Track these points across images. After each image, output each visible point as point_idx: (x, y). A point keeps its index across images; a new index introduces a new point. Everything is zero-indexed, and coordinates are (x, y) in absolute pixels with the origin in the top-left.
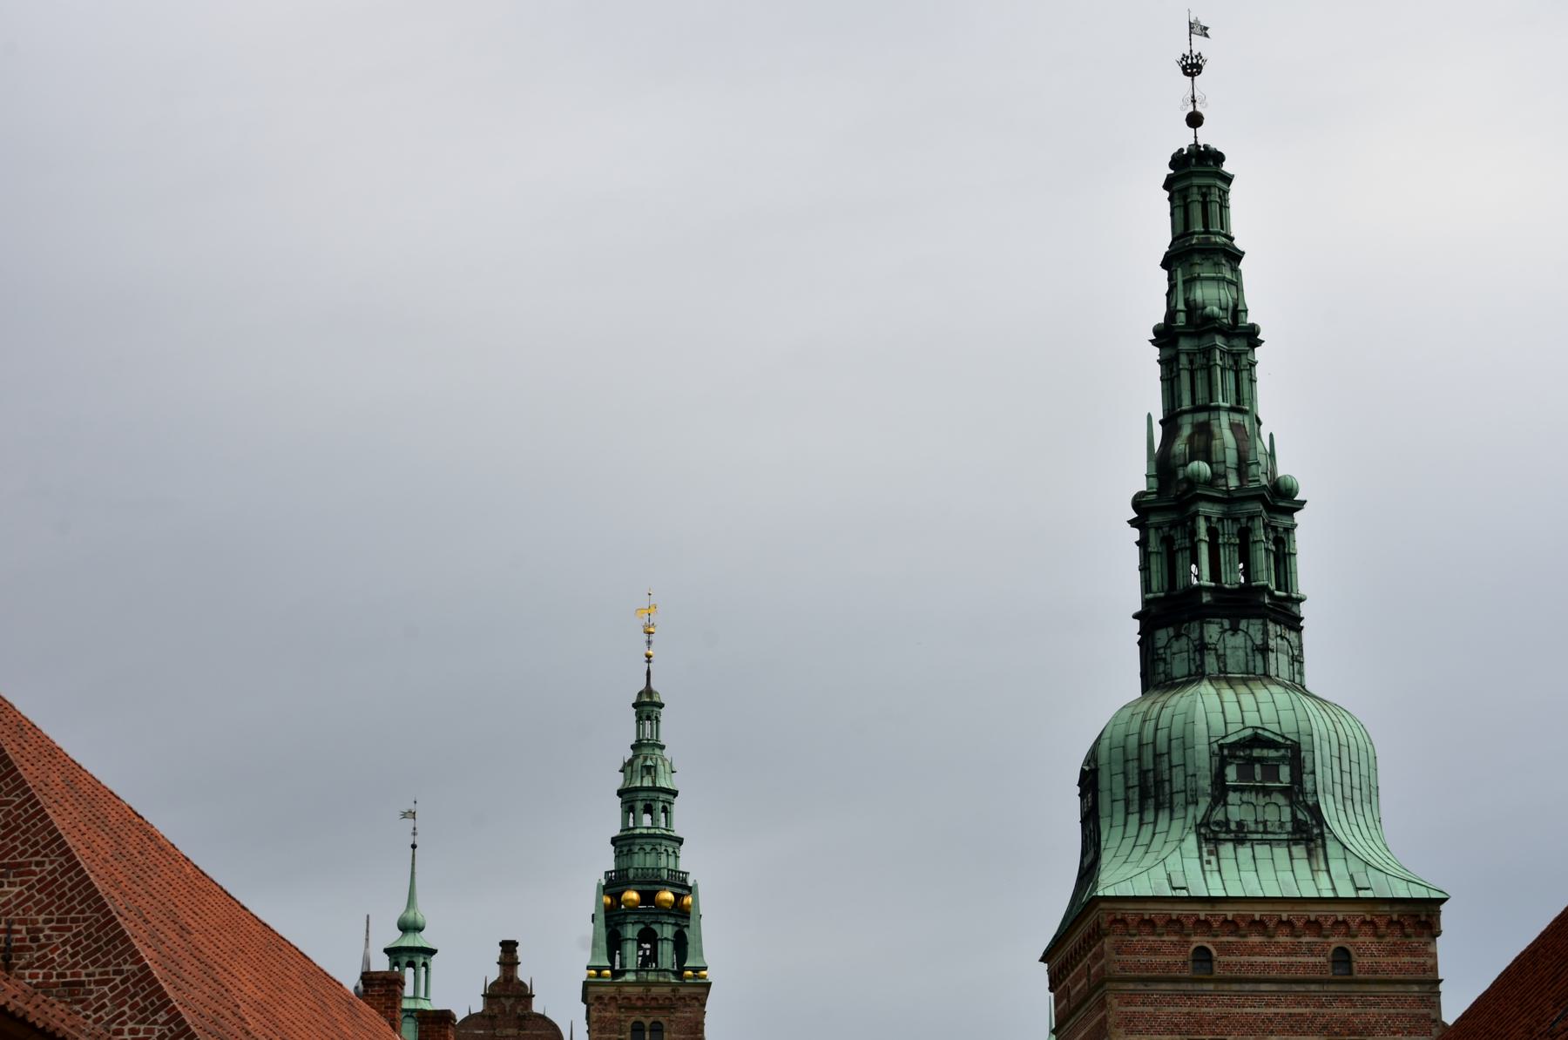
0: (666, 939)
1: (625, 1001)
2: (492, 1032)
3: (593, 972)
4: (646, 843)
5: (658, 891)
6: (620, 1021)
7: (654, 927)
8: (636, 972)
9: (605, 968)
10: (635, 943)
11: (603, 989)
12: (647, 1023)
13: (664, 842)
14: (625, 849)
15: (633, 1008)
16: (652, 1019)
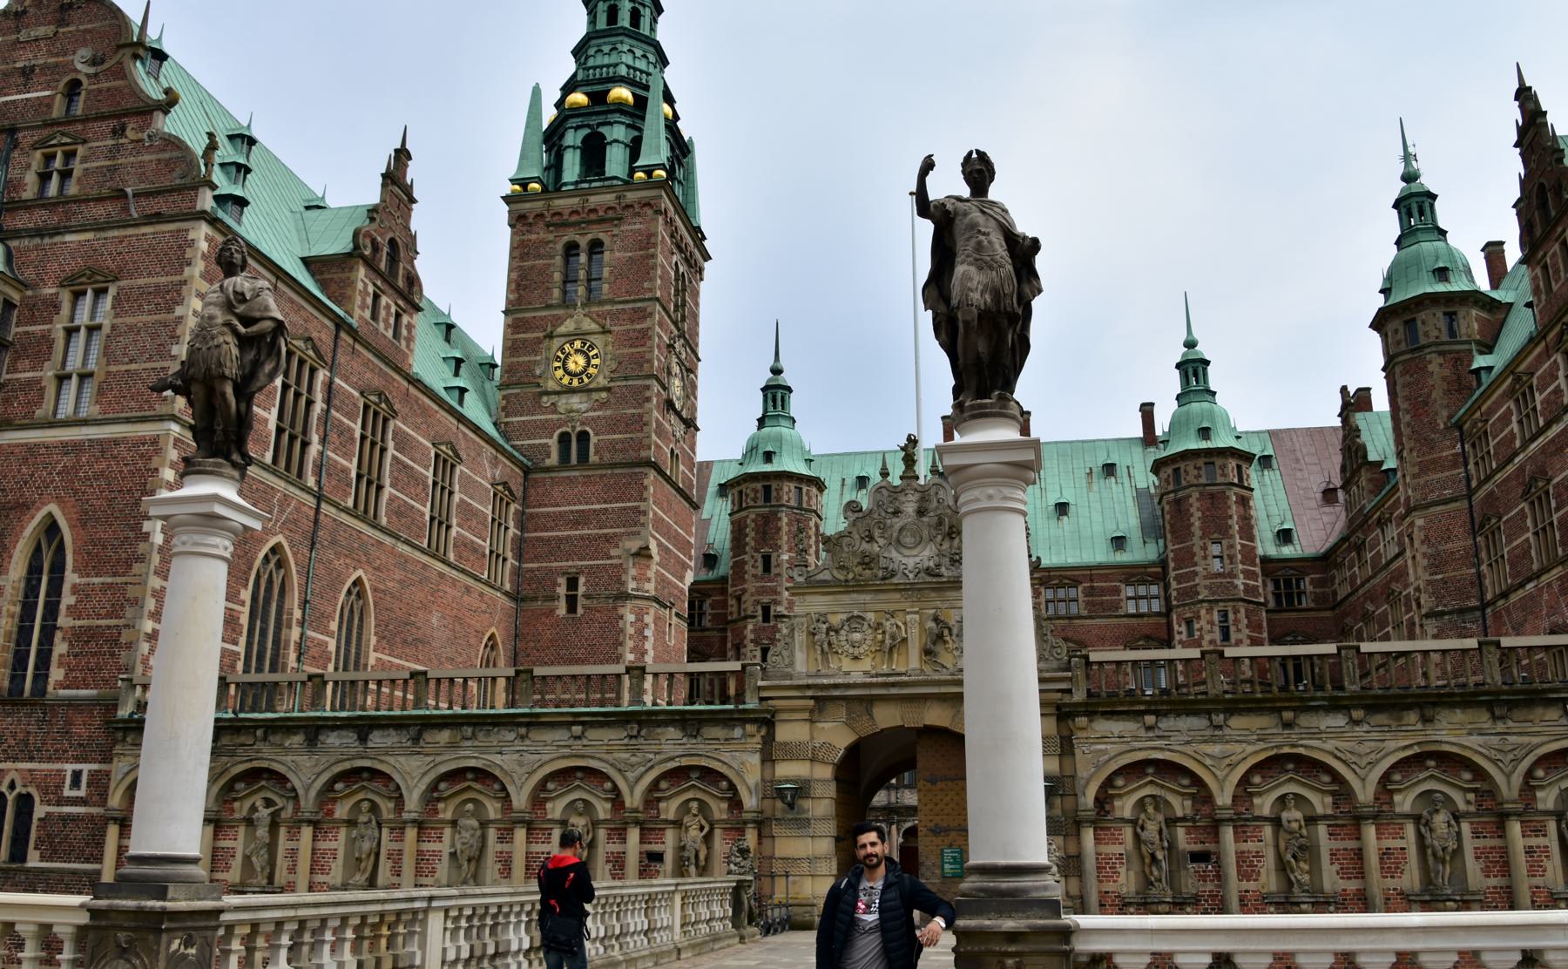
0: (616, 141)
1: (556, 218)
2: (14, 37)
3: (517, 187)
4: (605, 43)
5: (609, 91)
6: (548, 242)
7: (602, 130)
8: (576, 183)
9: (532, 179)
10: (578, 151)
11: (528, 205)
12: (583, 242)
13: (626, 40)
14: (583, 60)
15: (565, 225)
16: (590, 237)
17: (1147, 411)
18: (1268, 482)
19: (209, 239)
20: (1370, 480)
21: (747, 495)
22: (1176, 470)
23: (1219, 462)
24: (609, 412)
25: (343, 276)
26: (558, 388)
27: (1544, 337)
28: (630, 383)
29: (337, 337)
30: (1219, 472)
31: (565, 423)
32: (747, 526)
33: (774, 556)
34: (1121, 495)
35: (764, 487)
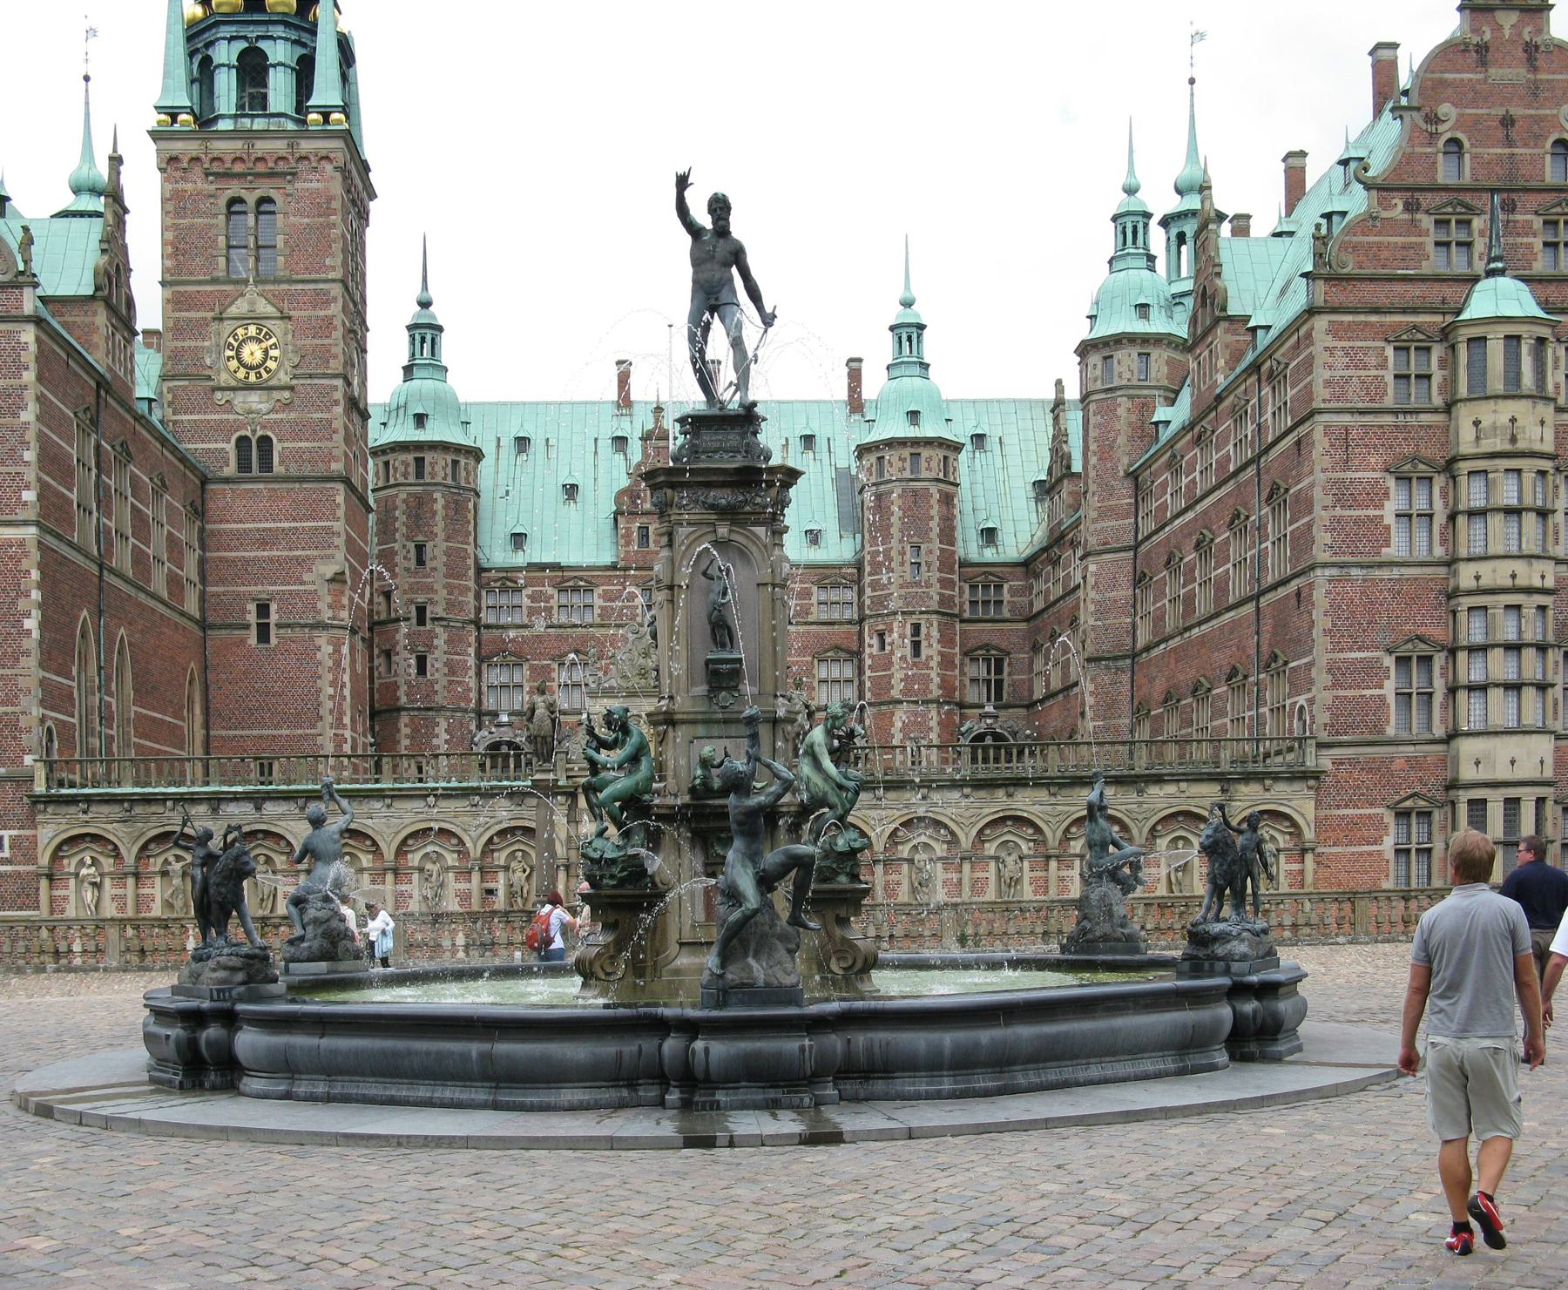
17: (855, 376)
18: (978, 467)
19: (38, 340)
20: (1070, 493)
21: (395, 469)
22: (880, 459)
23: (925, 453)
24: (293, 415)
25: (87, 320)
26: (234, 383)
27: (1192, 429)
28: (316, 381)
29: (98, 396)
30: (924, 465)
31: (243, 426)
32: (396, 508)
33: (429, 545)
34: (819, 475)
35: (416, 459)
